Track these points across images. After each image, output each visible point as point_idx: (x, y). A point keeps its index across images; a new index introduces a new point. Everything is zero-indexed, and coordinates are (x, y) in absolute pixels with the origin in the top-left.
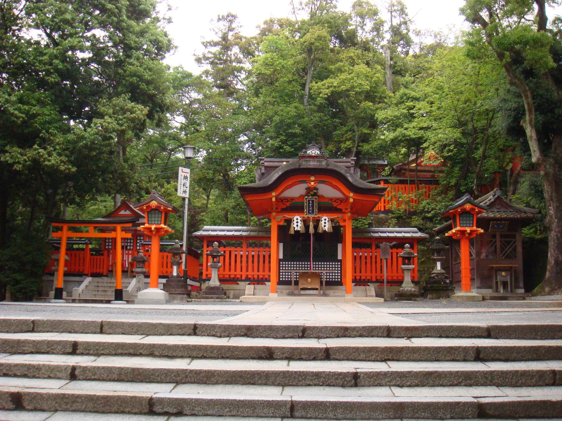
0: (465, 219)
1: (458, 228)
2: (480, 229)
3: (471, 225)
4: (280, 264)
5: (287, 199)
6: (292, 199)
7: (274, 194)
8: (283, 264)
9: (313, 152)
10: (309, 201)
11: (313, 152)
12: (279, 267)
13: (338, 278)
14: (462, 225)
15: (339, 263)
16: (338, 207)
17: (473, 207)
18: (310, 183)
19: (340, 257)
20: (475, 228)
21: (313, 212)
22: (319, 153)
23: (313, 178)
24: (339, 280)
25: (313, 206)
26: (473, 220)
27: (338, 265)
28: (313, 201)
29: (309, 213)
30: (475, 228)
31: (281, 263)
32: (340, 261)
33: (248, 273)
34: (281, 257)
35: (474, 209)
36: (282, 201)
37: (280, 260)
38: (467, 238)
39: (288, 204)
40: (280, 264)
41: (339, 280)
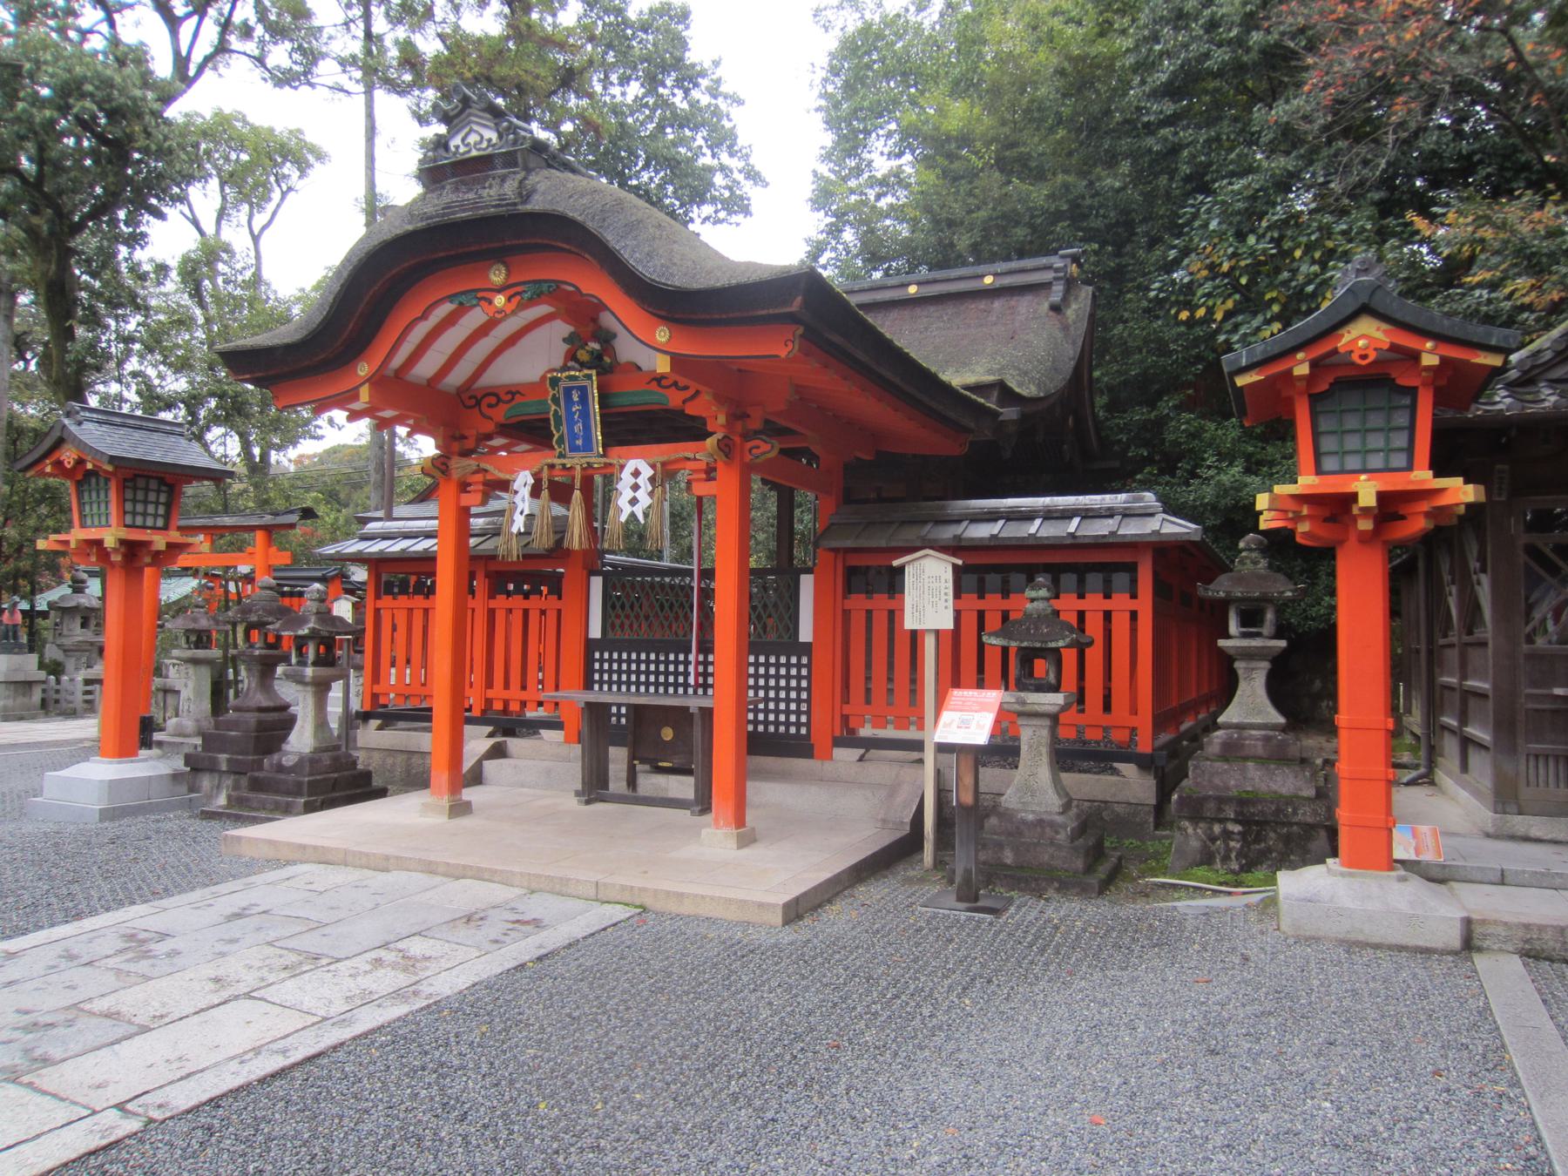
0: (1352, 422)
1: (1307, 482)
2: (1458, 481)
3: (1399, 460)
4: (589, 661)
5: (497, 395)
6: (513, 392)
7: (363, 370)
8: (602, 661)
9: (473, 138)
10: (568, 391)
11: (473, 138)
12: (589, 671)
13: (798, 724)
14: (1329, 463)
15: (805, 660)
16: (691, 410)
17: (1408, 341)
18: (491, 302)
19: (806, 634)
20: (1423, 476)
21: (588, 446)
22: (494, 136)
23: (497, 276)
24: (803, 731)
25: (585, 415)
26: (1412, 428)
27: (799, 666)
28: (583, 391)
29: (574, 449)
30: (1423, 476)
31: (597, 655)
32: (807, 649)
33: (490, 694)
34: (595, 632)
35: (1415, 356)
36: (478, 403)
37: (590, 645)
38: (1366, 539)
39: (502, 414)
40: (589, 661)
41: (803, 731)
